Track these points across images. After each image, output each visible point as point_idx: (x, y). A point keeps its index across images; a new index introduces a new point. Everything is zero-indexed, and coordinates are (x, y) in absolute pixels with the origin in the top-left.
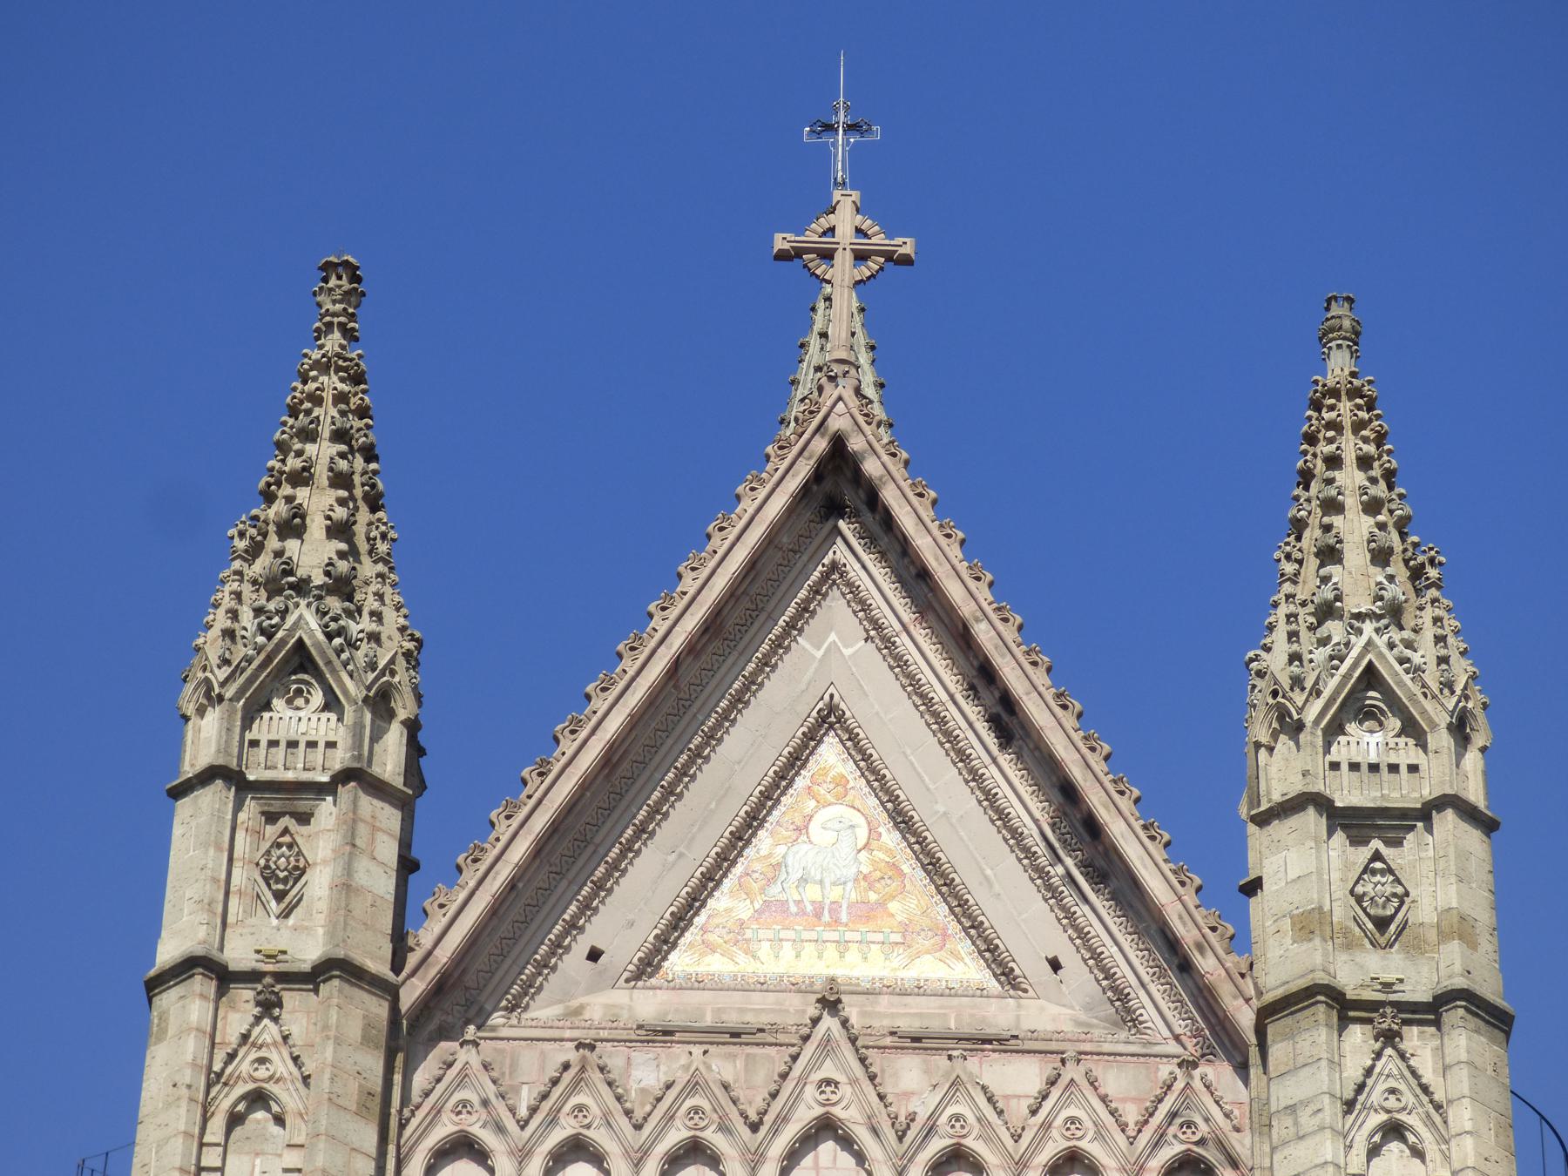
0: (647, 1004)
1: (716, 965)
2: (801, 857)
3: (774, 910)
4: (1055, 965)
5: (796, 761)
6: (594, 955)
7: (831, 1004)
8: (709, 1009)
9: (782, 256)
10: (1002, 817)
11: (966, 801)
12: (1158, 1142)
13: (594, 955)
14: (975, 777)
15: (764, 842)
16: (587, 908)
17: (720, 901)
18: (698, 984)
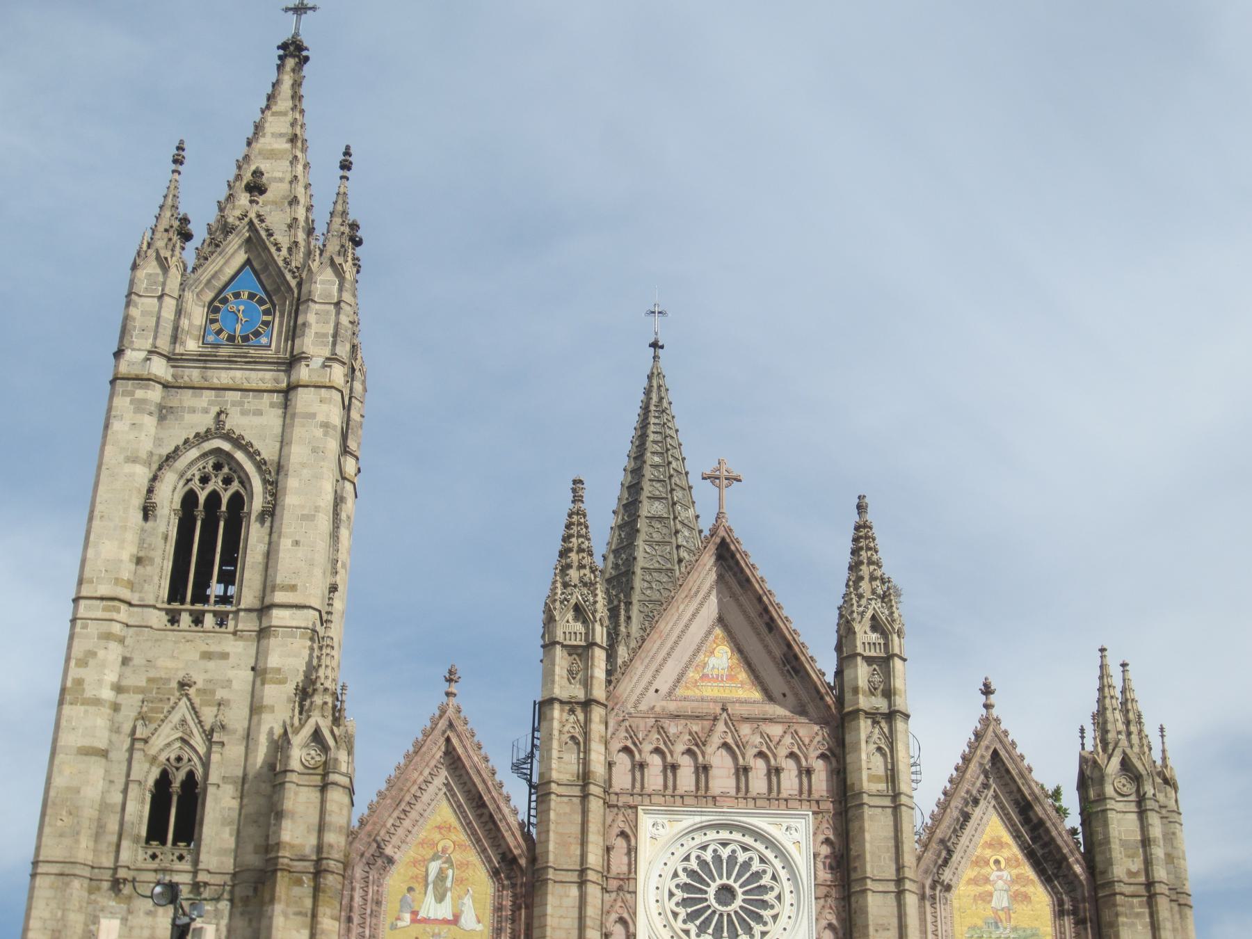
0: (672, 706)
1: (689, 693)
2: (712, 661)
3: (704, 677)
4: (784, 695)
5: (709, 633)
6: (657, 691)
7: (724, 709)
8: (688, 707)
10: (770, 652)
11: (759, 647)
13: (657, 691)
14: (762, 640)
15: (701, 657)
16: (654, 677)
17: (692, 674)
18: (685, 699)
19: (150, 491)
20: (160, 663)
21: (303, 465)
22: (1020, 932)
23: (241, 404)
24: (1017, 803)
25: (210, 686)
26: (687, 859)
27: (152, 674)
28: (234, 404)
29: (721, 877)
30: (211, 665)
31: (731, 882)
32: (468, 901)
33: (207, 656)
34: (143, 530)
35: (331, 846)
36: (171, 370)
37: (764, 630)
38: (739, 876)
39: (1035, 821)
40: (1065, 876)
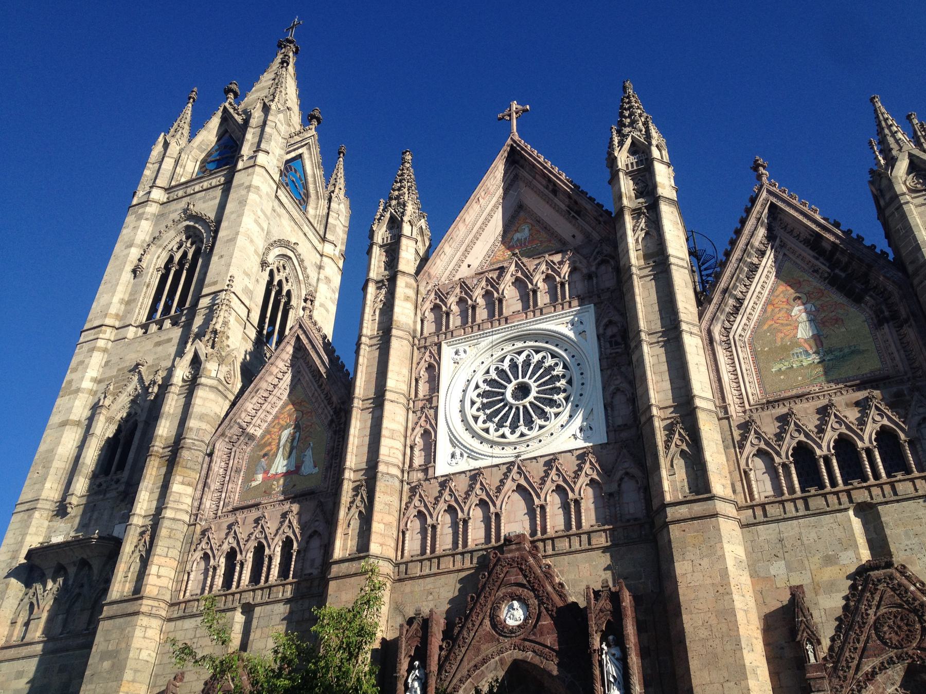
6: (469, 266)
9: (500, 119)
12: (595, 259)
13: (469, 266)
19: (140, 260)
20: (128, 357)
21: (232, 213)
22: (837, 353)
23: (204, 197)
24: (806, 242)
25: (157, 362)
26: (488, 372)
27: (120, 367)
28: (200, 199)
29: (517, 378)
30: (161, 347)
31: (526, 380)
32: (309, 453)
33: (158, 344)
34: (135, 285)
35: (191, 429)
36: (167, 196)
37: (551, 196)
38: (533, 374)
39: (829, 248)
40: (875, 288)
